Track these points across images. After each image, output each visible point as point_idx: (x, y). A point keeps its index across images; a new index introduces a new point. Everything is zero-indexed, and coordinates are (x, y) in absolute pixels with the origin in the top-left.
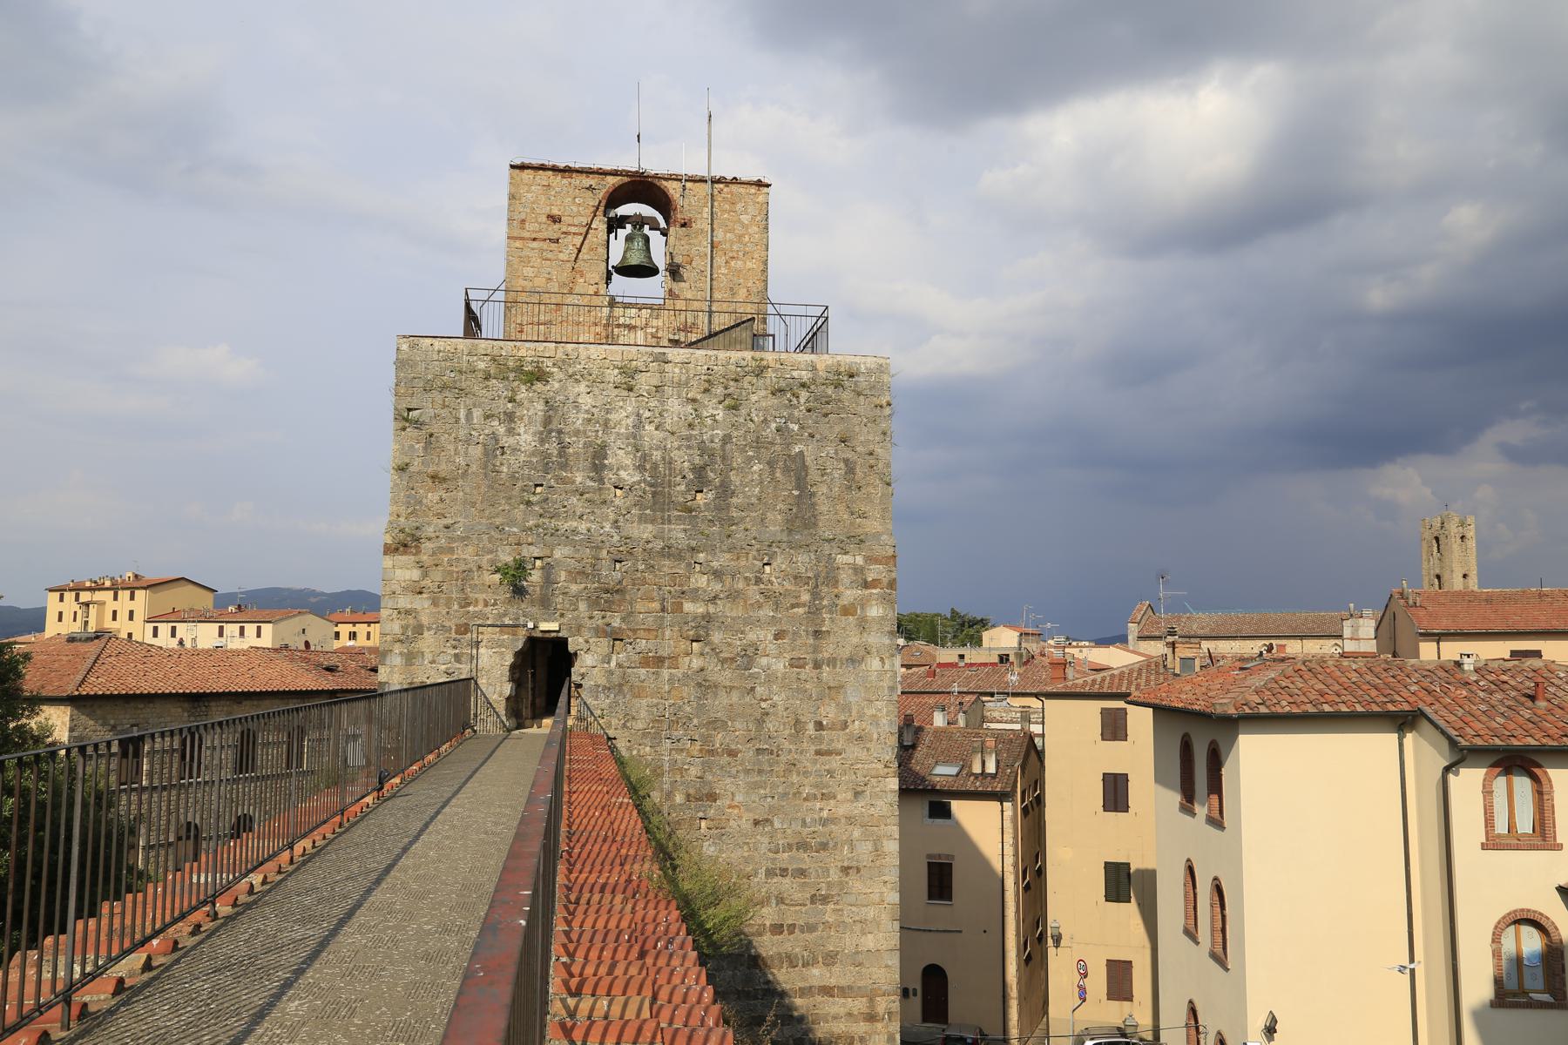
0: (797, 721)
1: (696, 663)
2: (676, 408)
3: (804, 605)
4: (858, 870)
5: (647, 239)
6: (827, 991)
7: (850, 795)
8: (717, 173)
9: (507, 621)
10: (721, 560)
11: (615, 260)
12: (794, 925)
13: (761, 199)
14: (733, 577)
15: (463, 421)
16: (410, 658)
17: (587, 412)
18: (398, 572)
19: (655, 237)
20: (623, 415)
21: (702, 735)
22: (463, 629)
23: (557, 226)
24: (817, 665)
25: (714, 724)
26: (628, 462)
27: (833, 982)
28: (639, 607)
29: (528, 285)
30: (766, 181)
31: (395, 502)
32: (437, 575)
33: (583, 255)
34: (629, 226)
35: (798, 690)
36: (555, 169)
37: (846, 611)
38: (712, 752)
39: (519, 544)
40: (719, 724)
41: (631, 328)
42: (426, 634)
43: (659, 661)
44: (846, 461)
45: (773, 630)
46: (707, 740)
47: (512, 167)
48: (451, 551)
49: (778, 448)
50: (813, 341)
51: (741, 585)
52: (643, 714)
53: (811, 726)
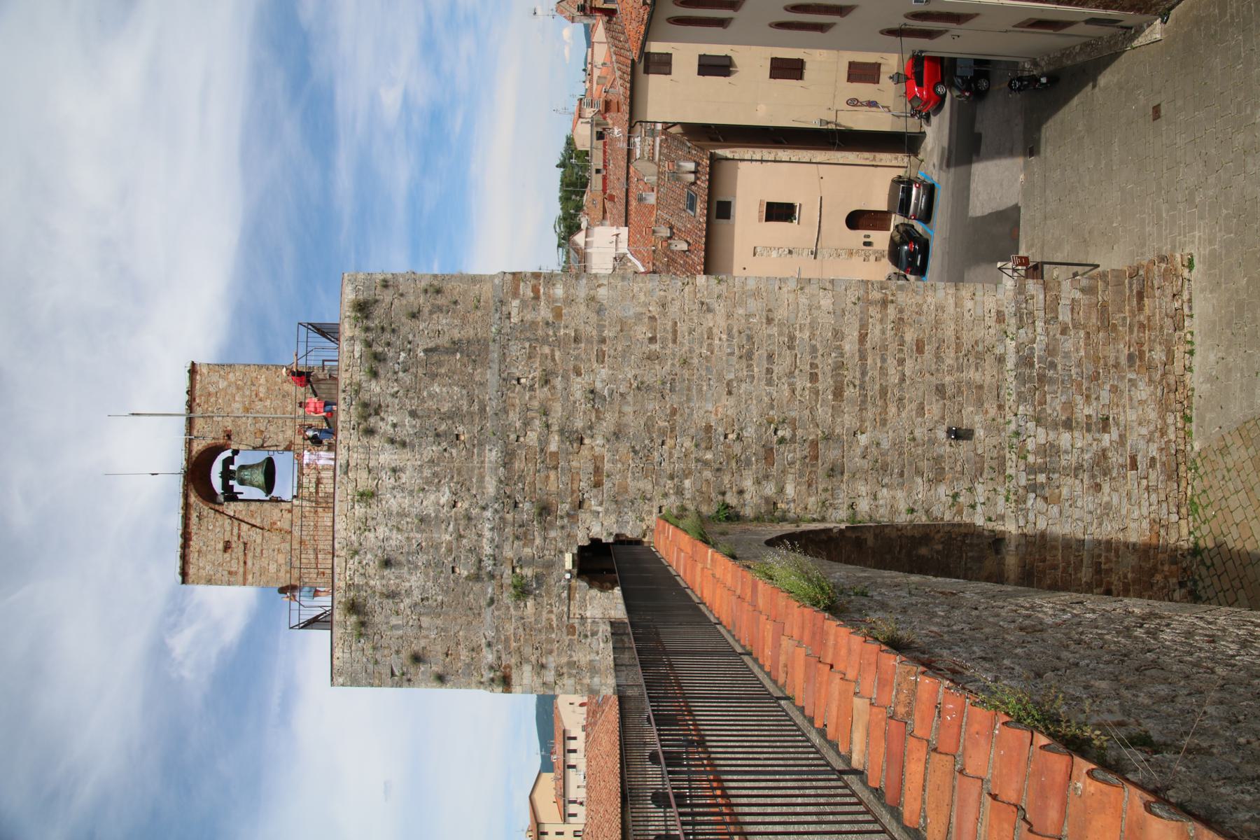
0: (648, 358)
1: (600, 441)
2: (388, 457)
3: (553, 351)
4: (770, 310)
5: (242, 467)
6: (863, 338)
7: (710, 316)
8: (182, 408)
9: (565, 594)
10: (514, 418)
11: (260, 494)
12: (812, 365)
13: (205, 371)
14: (528, 410)
15: (401, 632)
16: (593, 669)
17: (391, 530)
18: (525, 681)
19: (239, 461)
21: (658, 436)
22: (571, 629)
23: (234, 545)
24: (603, 341)
25: (648, 427)
26: (432, 497)
27: (856, 334)
28: (552, 487)
29: (283, 569)
30: (189, 366)
31: (468, 686)
32: (527, 650)
33: (258, 522)
34: (231, 482)
35: (623, 357)
36: (185, 545)
37: (558, 314)
39: (502, 586)
41: (318, 482)
42: (575, 659)
43: (597, 470)
44: (431, 313)
45: (572, 376)
46: (663, 432)
47: (184, 582)
48: (507, 640)
49: (421, 371)
50: (327, 332)
51: (536, 404)
52: (641, 485)
53: (653, 347)
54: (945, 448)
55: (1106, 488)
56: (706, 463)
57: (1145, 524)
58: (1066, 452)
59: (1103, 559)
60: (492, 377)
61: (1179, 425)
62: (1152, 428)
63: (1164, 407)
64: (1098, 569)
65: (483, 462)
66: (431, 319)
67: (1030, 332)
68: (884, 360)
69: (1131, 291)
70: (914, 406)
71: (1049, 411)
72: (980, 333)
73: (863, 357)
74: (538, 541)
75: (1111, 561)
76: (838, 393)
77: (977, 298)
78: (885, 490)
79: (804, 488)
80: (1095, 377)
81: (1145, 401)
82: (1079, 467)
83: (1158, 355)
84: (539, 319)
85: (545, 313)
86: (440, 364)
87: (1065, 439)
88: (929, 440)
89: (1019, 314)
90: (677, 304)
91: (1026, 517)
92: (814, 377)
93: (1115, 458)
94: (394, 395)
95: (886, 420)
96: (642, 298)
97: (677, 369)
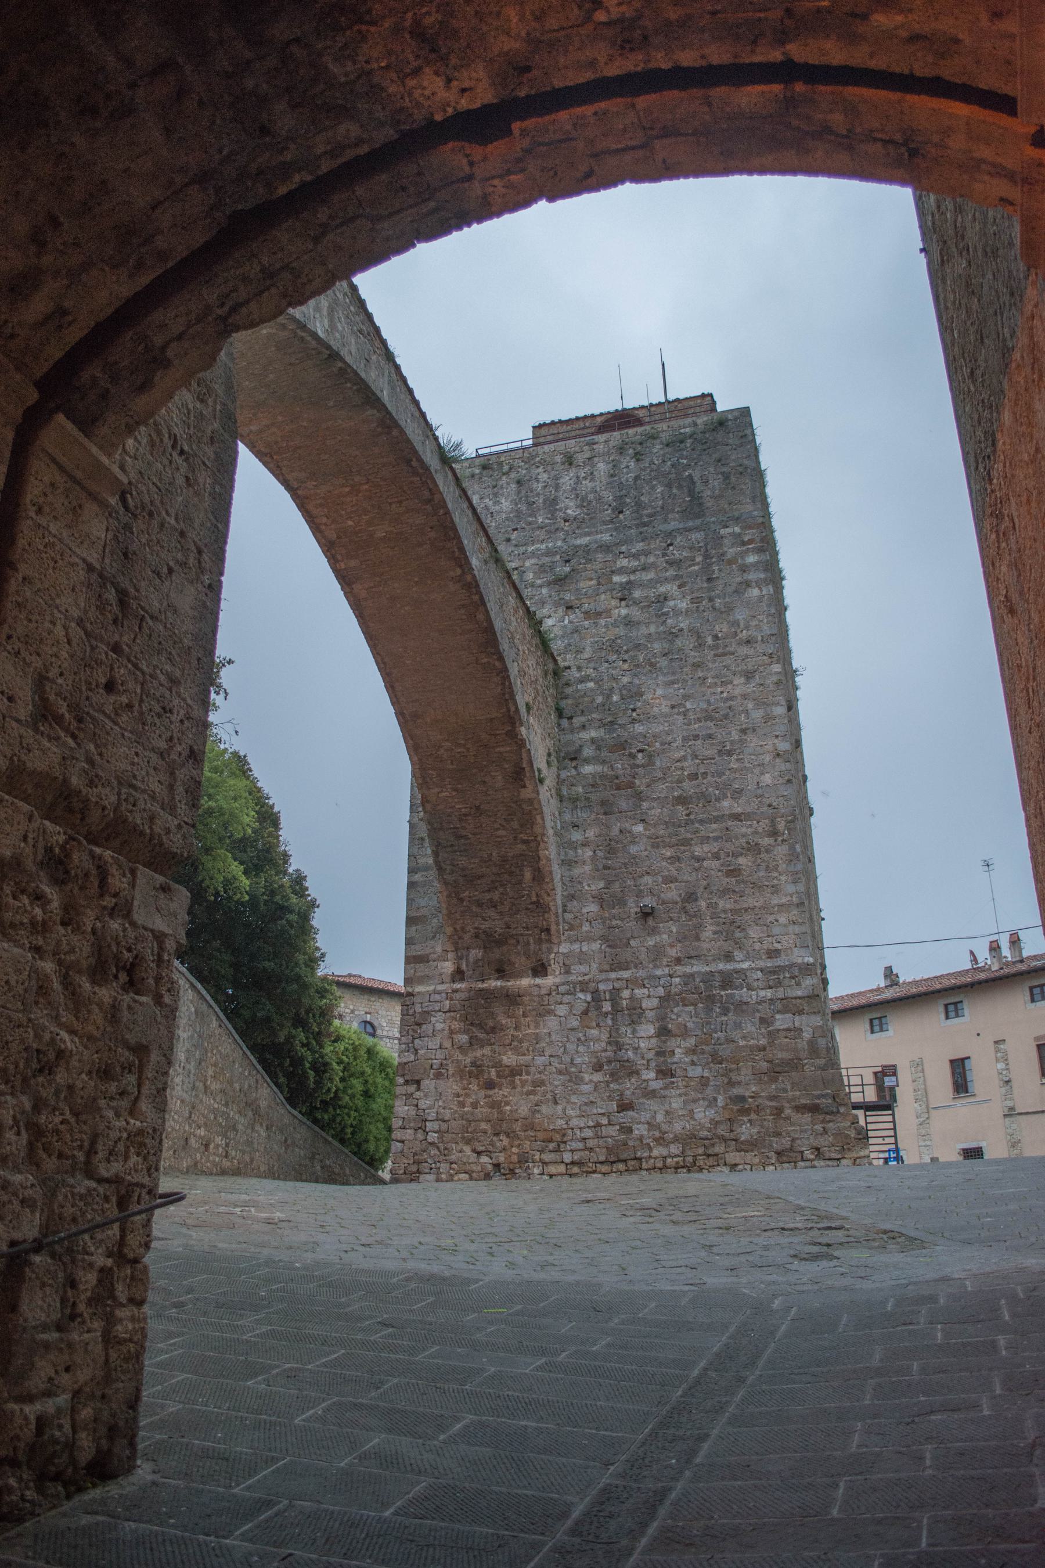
3: (698, 564)
4: (754, 730)
6: (737, 817)
20: (567, 481)
27: (740, 810)
37: (730, 562)
38: (637, 666)
40: (642, 647)
43: (599, 614)
44: (723, 473)
45: (677, 583)
46: (633, 658)
52: (588, 649)
54: (633, 907)
55: (598, 1077)
56: (609, 697)
57: (561, 1123)
58: (634, 1031)
59: (525, 1077)
60: (673, 525)
61: (669, 1160)
62: (665, 1127)
63: (689, 1139)
64: (514, 1072)
65: (601, 533)
66: (717, 474)
67: (760, 984)
68: (716, 839)
69: (818, 1097)
70: (674, 873)
71: (676, 1010)
72: (754, 932)
73: (716, 820)
74: (539, 582)
75: (522, 1087)
76: (682, 800)
77: (791, 928)
78: (591, 853)
79: (591, 781)
80: (716, 1059)
81: (692, 1118)
82: (619, 1047)
83: (746, 1131)
84: (725, 549)
85: (731, 552)
86: (680, 487)
87: (647, 1029)
88: (641, 891)
89: (774, 971)
90: (751, 652)
91: (568, 993)
92: (694, 776)
93: (629, 1086)
94: (652, 463)
95: (658, 847)
96: (754, 623)
97: (690, 660)
